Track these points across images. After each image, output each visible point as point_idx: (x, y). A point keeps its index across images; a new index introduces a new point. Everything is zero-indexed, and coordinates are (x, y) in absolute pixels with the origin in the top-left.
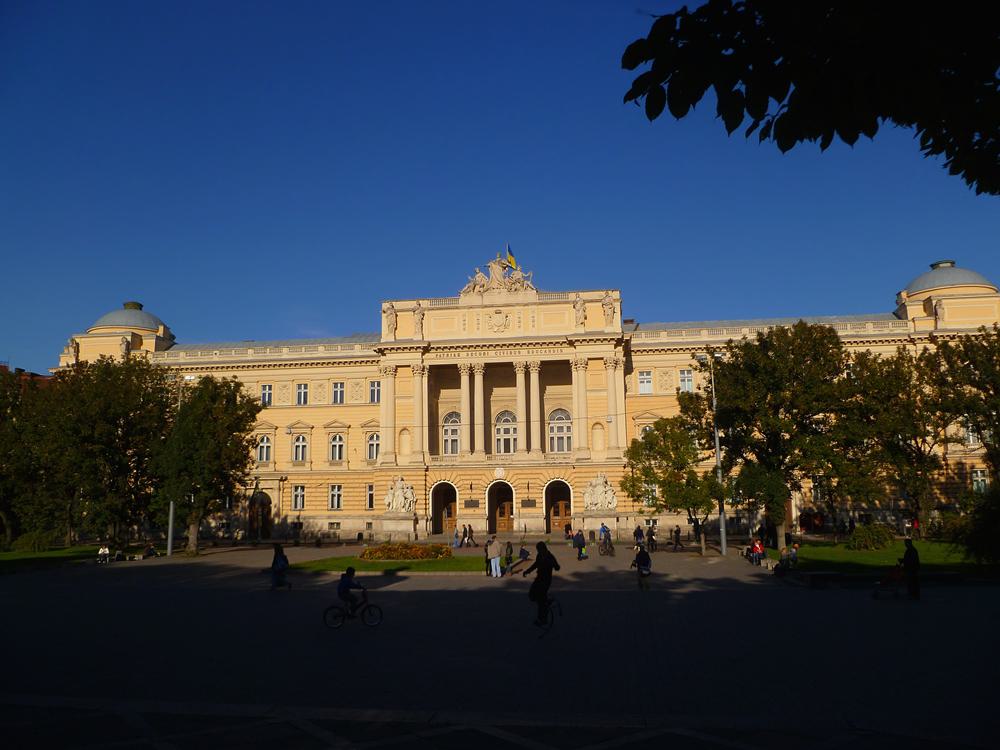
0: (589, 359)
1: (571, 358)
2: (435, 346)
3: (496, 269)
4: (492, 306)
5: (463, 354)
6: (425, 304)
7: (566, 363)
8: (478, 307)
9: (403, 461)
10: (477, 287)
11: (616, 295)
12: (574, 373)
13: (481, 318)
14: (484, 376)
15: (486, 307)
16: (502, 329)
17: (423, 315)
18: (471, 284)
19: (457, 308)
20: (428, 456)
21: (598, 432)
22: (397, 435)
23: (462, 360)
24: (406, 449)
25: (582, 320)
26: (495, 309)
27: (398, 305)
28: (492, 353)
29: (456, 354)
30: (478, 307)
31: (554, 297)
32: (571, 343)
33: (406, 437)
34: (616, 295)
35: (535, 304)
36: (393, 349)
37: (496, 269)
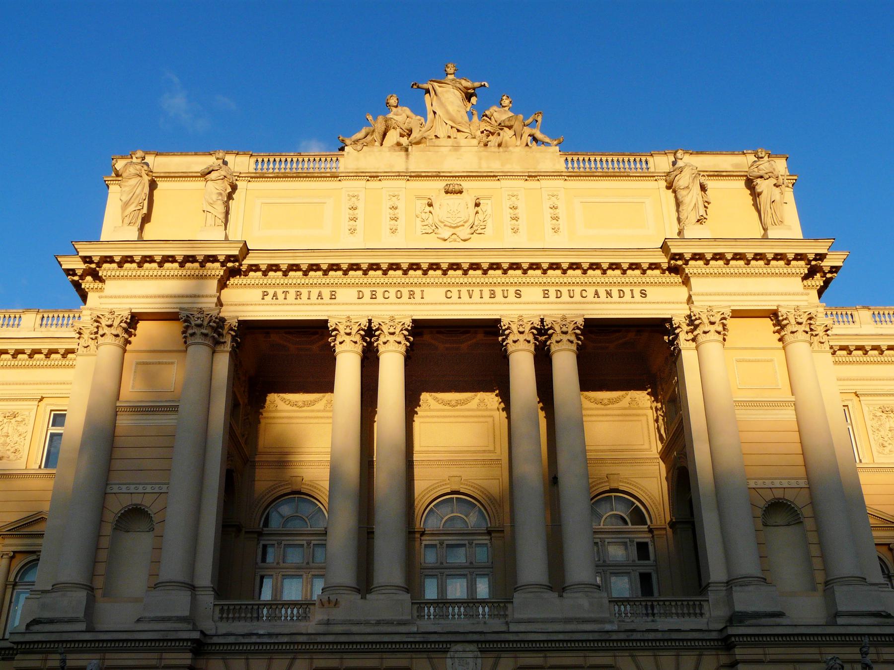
0: (737, 314)
1: (677, 313)
2: (264, 262)
3: (448, 99)
4: (437, 176)
5: (346, 295)
6: (241, 163)
7: (659, 330)
8: (399, 175)
9: (117, 617)
10: (393, 136)
11: (780, 166)
12: (688, 356)
13: (401, 205)
14: (410, 358)
15: (418, 176)
16: (464, 232)
17: (234, 188)
18: (380, 126)
19: (334, 176)
20: (207, 599)
21: (783, 538)
22: (108, 529)
23: (342, 307)
24: (133, 578)
25: (702, 212)
26: (441, 184)
27: (160, 163)
28: (435, 294)
29: (326, 292)
30: (399, 175)
31: (611, 162)
32: (676, 266)
33: (137, 544)
34: (780, 166)
35: (557, 175)
36: (128, 259)
37: (448, 99)
